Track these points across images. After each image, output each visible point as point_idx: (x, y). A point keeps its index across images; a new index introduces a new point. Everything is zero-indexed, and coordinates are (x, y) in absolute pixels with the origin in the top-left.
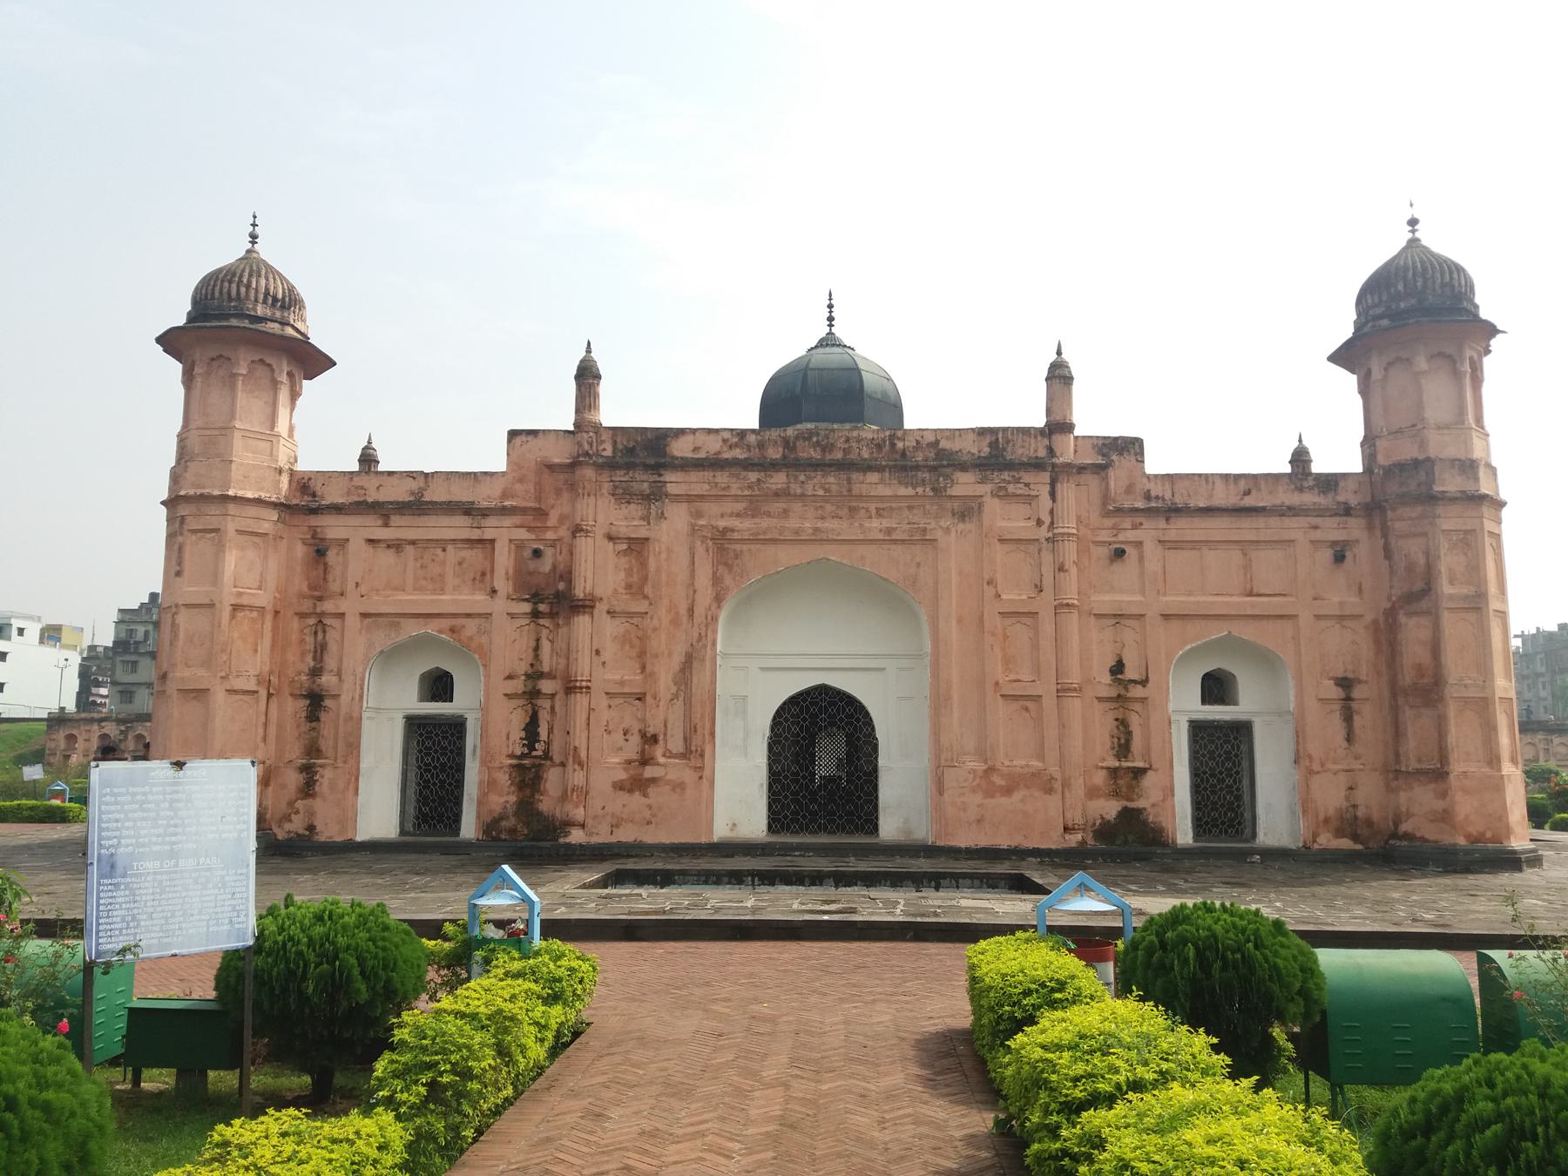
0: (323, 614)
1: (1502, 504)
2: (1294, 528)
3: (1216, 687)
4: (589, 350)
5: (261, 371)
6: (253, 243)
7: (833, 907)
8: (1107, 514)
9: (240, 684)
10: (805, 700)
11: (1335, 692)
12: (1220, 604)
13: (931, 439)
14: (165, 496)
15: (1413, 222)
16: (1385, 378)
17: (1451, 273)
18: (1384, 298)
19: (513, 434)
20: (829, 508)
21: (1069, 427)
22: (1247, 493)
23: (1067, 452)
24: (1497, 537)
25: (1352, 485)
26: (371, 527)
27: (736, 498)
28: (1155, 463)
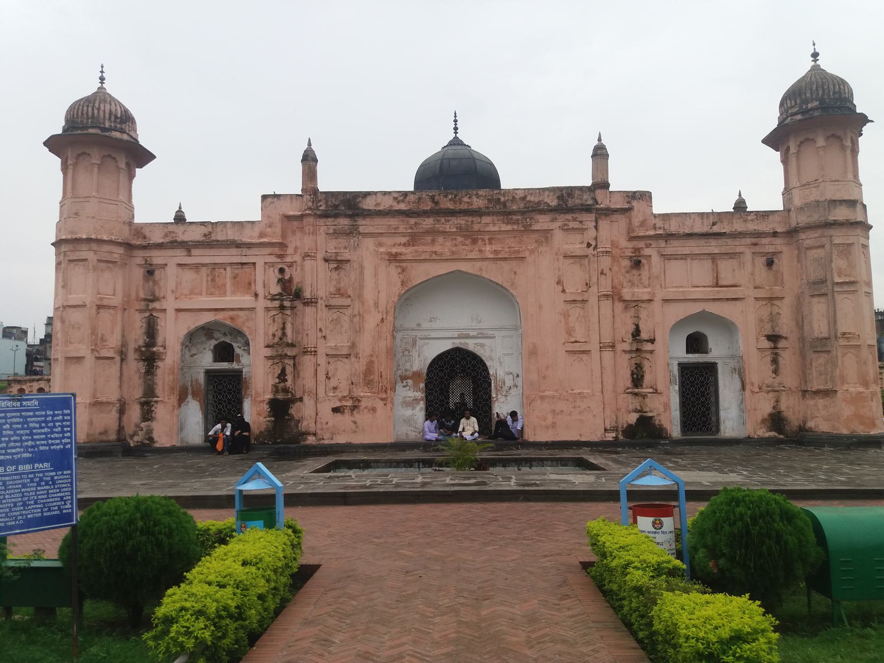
0: (154, 309)
1: (871, 227)
2: (741, 246)
3: (696, 343)
4: (310, 144)
6: (102, 83)
7: (472, 481)
8: (631, 239)
9: (104, 353)
10: (447, 357)
11: (767, 344)
12: (699, 293)
13: (522, 195)
14: (54, 240)
15: (815, 55)
16: (798, 152)
17: (839, 85)
18: (798, 101)
19: (264, 197)
20: (460, 239)
21: (606, 185)
22: (714, 224)
23: (604, 202)
24: (865, 247)
26: (180, 256)
27: (404, 235)
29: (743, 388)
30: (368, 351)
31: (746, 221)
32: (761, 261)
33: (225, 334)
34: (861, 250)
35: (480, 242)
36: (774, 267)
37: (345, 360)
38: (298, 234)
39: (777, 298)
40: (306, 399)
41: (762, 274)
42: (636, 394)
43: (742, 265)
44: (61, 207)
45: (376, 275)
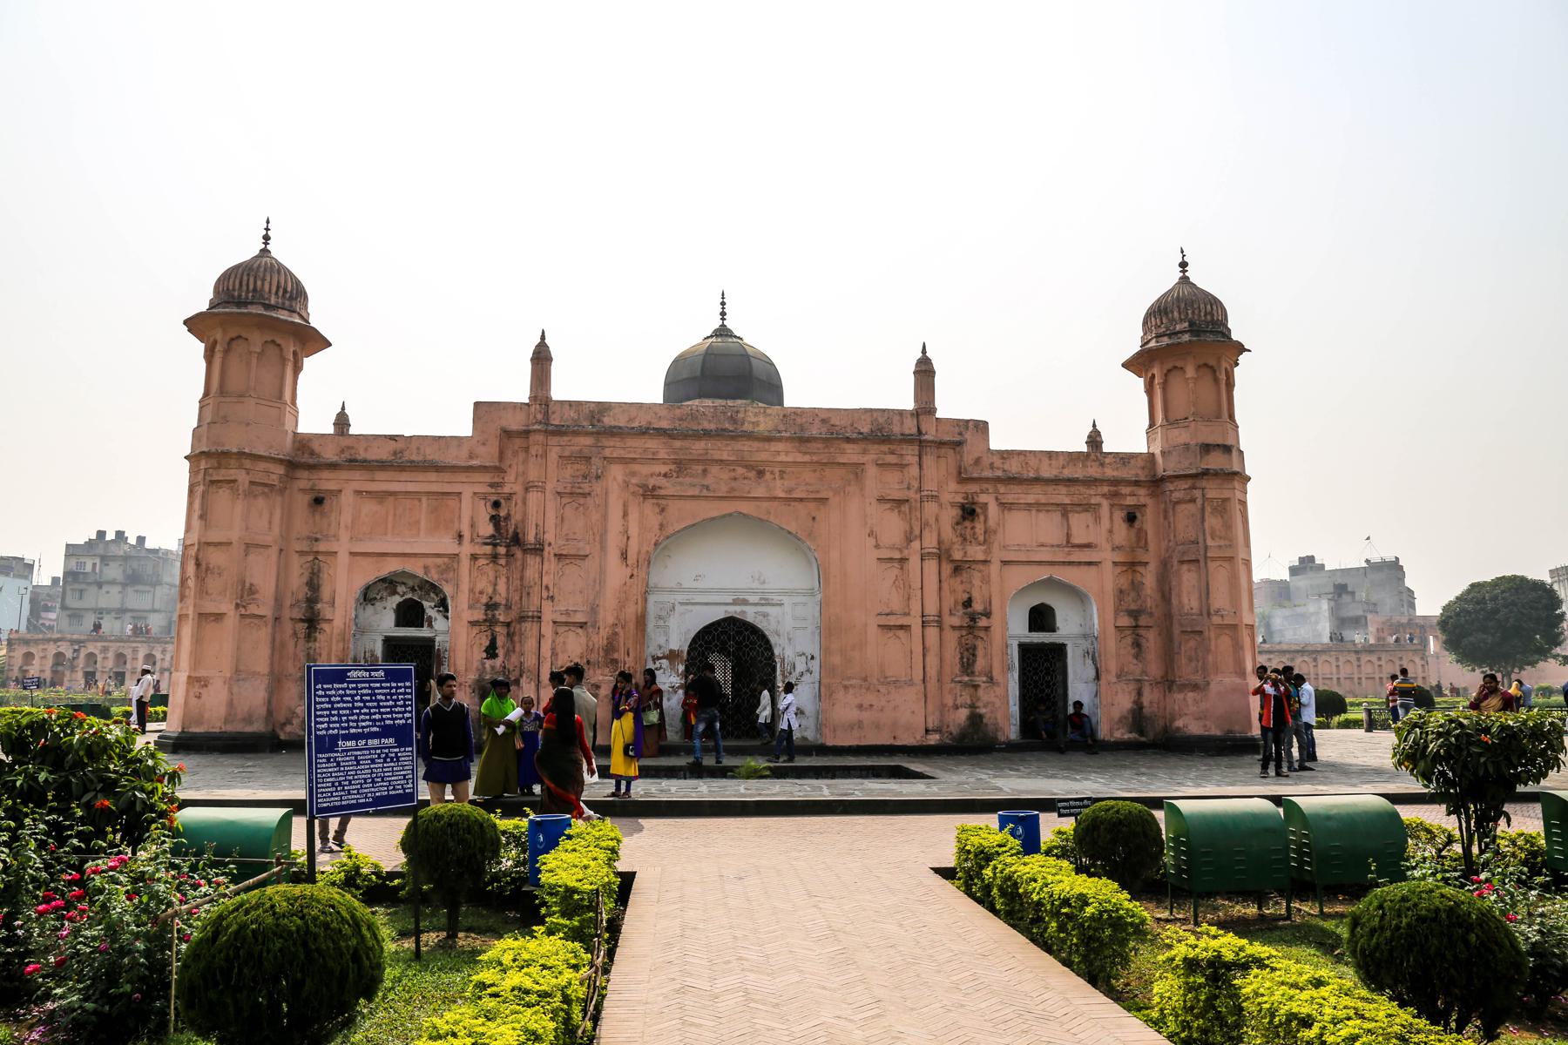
2: (1095, 496)
3: (1041, 618)
5: (272, 351)
6: (266, 244)
9: (253, 609)
11: (1125, 621)
14: (188, 452)
15: (1183, 265)
19: (477, 404)
20: (740, 471)
21: (932, 411)
24: (1244, 503)
25: (1140, 463)
26: (355, 481)
28: (997, 442)
29: (1098, 677)
30: (611, 620)
31: (1102, 465)
32: (1119, 515)
33: (413, 589)
34: (1238, 507)
35: (768, 476)
36: (1137, 524)
37: (580, 631)
38: (522, 456)
39: (1140, 563)
40: (523, 681)
41: (1122, 533)
42: (966, 685)
43: (1098, 519)
44: (201, 408)
45: (625, 515)
